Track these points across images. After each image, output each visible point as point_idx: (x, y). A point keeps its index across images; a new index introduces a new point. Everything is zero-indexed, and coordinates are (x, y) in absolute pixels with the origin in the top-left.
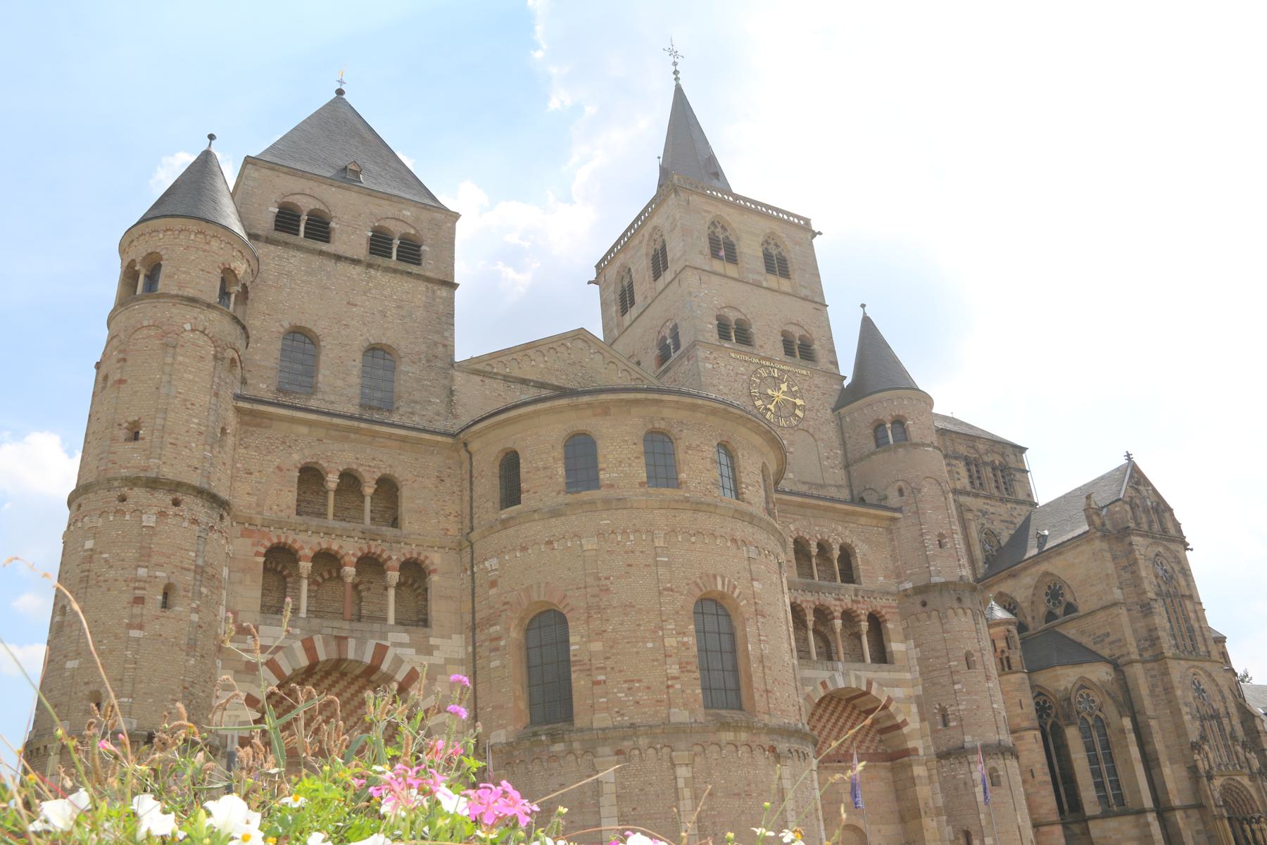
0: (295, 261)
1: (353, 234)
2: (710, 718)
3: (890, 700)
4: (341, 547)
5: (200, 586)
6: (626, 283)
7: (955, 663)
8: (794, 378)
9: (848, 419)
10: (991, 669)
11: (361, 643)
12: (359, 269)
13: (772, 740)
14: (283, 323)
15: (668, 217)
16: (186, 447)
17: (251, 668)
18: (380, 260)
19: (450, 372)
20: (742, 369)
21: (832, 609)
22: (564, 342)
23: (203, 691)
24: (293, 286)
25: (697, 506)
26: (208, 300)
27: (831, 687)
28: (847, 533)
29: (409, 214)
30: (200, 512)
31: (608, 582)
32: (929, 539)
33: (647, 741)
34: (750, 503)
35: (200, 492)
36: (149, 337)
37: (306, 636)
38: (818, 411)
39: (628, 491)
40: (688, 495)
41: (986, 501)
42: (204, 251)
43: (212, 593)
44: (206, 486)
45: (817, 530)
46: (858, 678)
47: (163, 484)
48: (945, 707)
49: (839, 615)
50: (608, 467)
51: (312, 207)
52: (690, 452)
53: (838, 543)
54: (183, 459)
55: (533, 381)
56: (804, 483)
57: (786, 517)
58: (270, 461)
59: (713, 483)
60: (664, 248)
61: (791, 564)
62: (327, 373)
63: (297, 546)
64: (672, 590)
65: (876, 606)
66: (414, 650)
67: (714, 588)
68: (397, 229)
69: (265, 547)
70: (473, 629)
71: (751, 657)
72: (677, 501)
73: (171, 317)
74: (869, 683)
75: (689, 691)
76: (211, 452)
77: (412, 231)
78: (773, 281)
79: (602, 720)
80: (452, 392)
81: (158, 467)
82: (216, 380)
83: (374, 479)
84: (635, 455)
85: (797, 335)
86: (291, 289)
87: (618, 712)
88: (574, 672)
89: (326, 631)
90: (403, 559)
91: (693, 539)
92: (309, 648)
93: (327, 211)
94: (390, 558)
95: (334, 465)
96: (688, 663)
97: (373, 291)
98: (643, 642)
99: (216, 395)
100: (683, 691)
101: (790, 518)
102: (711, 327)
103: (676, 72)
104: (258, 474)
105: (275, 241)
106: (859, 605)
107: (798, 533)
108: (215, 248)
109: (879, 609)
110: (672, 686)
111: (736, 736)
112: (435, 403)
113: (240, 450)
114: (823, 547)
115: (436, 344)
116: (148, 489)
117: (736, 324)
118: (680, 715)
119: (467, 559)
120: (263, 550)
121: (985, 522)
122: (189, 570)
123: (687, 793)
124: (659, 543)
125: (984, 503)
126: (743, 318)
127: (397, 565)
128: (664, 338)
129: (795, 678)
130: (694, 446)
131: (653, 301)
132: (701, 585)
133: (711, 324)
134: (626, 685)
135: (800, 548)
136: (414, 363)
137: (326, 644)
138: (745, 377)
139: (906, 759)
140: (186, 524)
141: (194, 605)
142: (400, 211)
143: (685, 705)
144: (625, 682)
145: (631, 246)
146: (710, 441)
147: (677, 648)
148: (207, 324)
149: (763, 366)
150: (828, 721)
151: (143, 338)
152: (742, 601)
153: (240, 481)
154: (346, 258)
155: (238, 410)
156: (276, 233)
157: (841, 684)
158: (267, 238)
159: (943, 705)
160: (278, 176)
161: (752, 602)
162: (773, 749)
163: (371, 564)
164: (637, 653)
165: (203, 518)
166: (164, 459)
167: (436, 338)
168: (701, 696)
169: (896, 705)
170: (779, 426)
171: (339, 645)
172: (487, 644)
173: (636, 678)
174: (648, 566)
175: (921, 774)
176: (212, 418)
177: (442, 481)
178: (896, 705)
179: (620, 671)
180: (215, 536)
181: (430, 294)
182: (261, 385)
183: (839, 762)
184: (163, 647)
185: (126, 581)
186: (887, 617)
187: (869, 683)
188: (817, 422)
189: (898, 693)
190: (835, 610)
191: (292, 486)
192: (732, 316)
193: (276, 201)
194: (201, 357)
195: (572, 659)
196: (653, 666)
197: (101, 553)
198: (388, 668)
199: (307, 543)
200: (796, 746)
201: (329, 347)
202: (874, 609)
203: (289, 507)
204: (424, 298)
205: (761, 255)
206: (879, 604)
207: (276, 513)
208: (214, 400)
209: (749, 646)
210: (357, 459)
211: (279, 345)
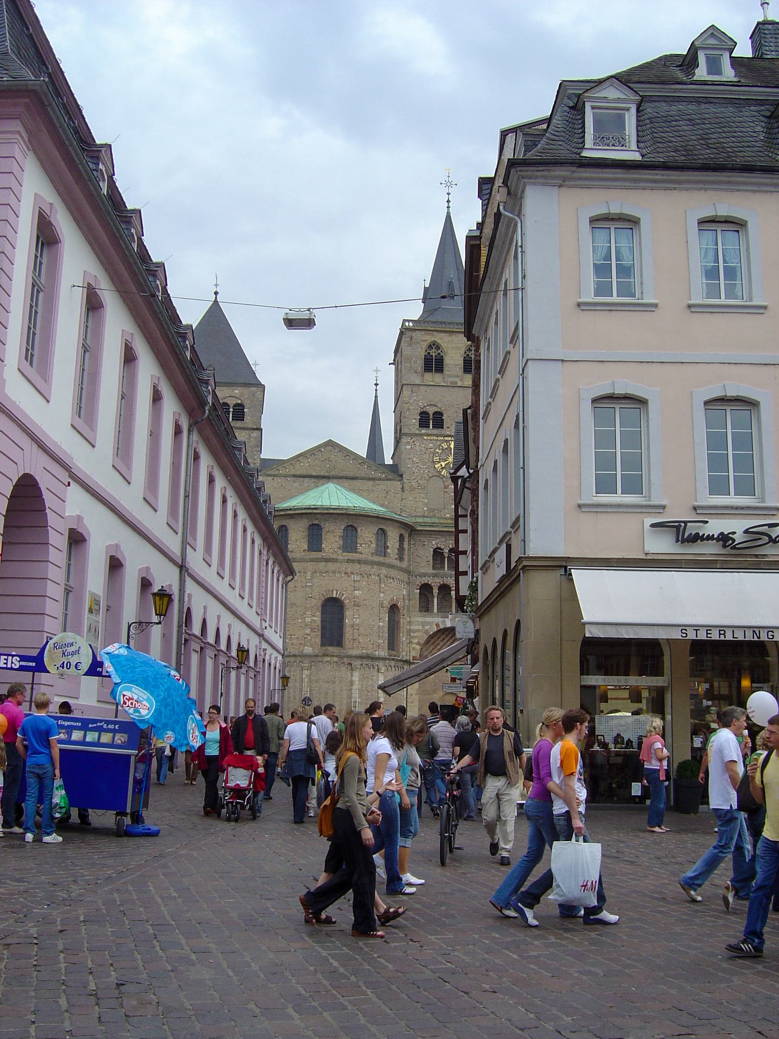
25: (327, 560)
59: (338, 548)
68: (232, 402)
77: (239, 402)
91: (324, 575)
102: (415, 421)
103: (448, 201)
118: (308, 650)
126: (439, 410)
138: (432, 450)
143: (311, 646)
161: (353, 600)
192: (431, 410)
200: (367, 663)
205: (461, 362)
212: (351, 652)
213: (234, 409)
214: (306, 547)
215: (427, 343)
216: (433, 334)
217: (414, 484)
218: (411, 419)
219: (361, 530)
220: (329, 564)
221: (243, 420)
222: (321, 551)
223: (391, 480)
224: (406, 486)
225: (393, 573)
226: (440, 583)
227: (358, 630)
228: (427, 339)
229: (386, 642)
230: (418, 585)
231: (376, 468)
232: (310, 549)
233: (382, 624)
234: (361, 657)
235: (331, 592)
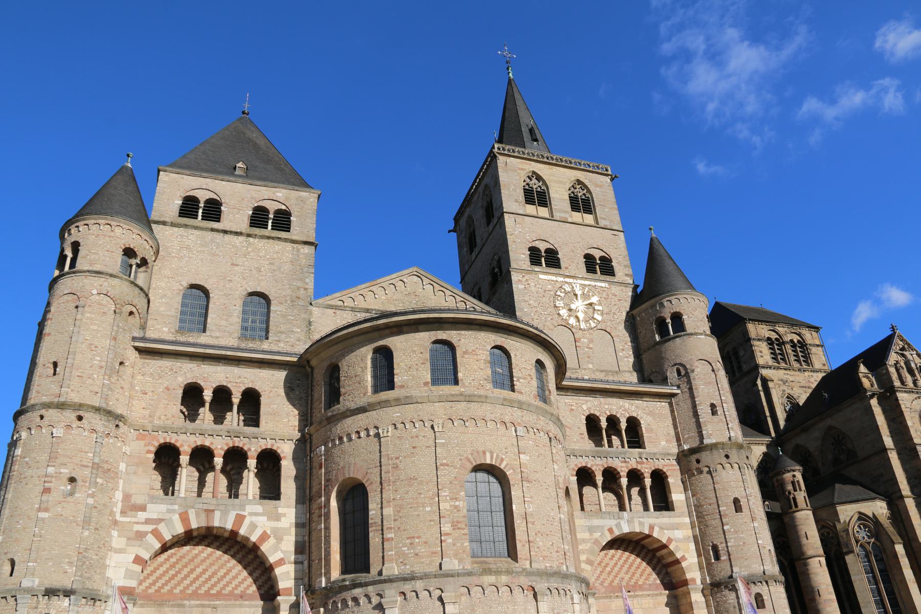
0: (192, 237)
1: (237, 214)
2: (476, 565)
3: (670, 540)
4: (212, 443)
5: (96, 478)
6: (472, 229)
7: (725, 508)
8: (593, 289)
9: (638, 318)
10: (756, 511)
11: (225, 513)
12: (241, 238)
13: (531, 581)
14: (182, 283)
15: (492, 177)
16: (89, 378)
17: (140, 535)
18: (257, 231)
19: (310, 308)
21: (619, 470)
22: (401, 278)
23: (97, 555)
24: (191, 255)
26: (111, 272)
27: (617, 533)
28: (633, 408)
29: (281, 195)
30: (98, 424)
31: (398, 461)
32: (702, 409)
33: (422, 585)
34: (521, 393)
35: (97, 410)
36: (67, 301)
37: (183, 511)
38: (614, 314)
39: (415, 390)
40: (464, 390)
41: (786, 372)
42: (110, 237)
43: (107, 482)
44: (104, 406)
45: (603, 408)
46: (641, 524)
47: (69, 405)
48: (716, 545)
49: (626, 474)
50: (401, 372)
51: (208, 198)
52: (466, 356)
53: (624, 417)
54: (86, 387)
55: (375, 310)
56: (602, 371)
57: (579, 400)
58: (161, 384)
59: (485, 379)
60: (491, 200)
61: (583, 436)
62: (214, 316)
63: (178, 444)
64: (448, 465)
65: (658, 465)
66: (266, 518)
67: (483, 462)
68: (272, 207)
69: (155, 446)
70: (310, 500)
72: (453, 395)
73: (83, 286)
74: (652, 528)
75: (459, 545)
76: (109, 380)
77: (284, 207)
78: (577, 216)
79: (392, 569)
80: (310, 323)
81: (67, 394)
82: (115, 328)
83: (239, 392)
84: (421, 362)
85: (597, 257)
86: (189, 257)
87: (402, 562)
88: (372, 531)
89: (197, 506)
90: (260, 450)
92: (184, 518)
93: (218, 199)
94: (250, 449)
95: (209, 384)
96: (458, 522)
97: (252, 254)
98: (422, 507)
99: (115, 339)
100: (454, 545)
101: (584, 400)
104: (151, 394)
105: (178, 224)
106: (643, 466)
107: (589, 411)
108: (118, 234)
109: (661, 468)
111: (497, 579)
112: (297, 332)
113: (138, 377)
114: (613, 421)
115: (298, 288)
116: (59, 410)
117: (545, 252)
119: (308, 448)
120: (154, 449)
121: (785, 388)
122: (87, 466)
125: (784, 374)
126: (552, 247)
127: (256, 455)
128: (494, 269)
129: (561, 529)
131: (486, 241)
132: (472, 460)
133: (523, 254)
135: (592, 422)
136: (281, 304)
137: (197, 515)
138: (552, 293)
139: (685, 587)
140: (86, 433)
141: (90, 492)
142: (274, 193)
143: (455, 555)
144: (408, 538)
145: (473, 201)
146: (485, 346)
148: (109, 289)
149: (567, 283)
150: (620, 559)
151: (63, 303)
152: (510, 469)
153: (138, 400)
154: (231, 232)
155: (136, 348)
156: (180, 218)
157: (626, 529)
158: (172, 223)
159: (715, 543)
160: (183, 178)
163: (236, 457)
164: (418, 515)
165: (100, 428)
166: (72, 387)
167: (299, 284)
168: (468, 548)
169: (676, 544)
170: (580, 329)
171: (207, 516)
172: (317, 511)
173: (417, 535)
174: (429, 447)
175: (698, 600)
176: (111, 356)
177: (293, 390)
178: (676, 544)
179: (404, 530)
180: (111, 441)
181: (295, 252)
182: (164, 329)
183: (629, 592)
184: (63, 524)
185: (39, 477)
186: (668, 474)
187: (652, 528)
188: (614, 322)
189: (678, 534)
190: (622, 471)
191: (177, 401)
192: (543, 247)
193: (180, 196)
194: (104, 313)
195: (370, 521)
196: (430, 525)
197: (24, 458)
198: (245, 532)
199: (186, 444)
200: (556, 585)
201: (216, 297)
202: (657, 468)
203: (173, 416)
204: (290, 256)
205: (568, 198)
206: (659, 464)
207: (164, 421)
208: (113, 343)
210: (227, 378)
211: (179, 299)
214: (428, 377)
216: (531, 165)
221: (289, 231)
226: (602, 465)
228: (524, 167)
232: (436, 381)
235: (481, 454)
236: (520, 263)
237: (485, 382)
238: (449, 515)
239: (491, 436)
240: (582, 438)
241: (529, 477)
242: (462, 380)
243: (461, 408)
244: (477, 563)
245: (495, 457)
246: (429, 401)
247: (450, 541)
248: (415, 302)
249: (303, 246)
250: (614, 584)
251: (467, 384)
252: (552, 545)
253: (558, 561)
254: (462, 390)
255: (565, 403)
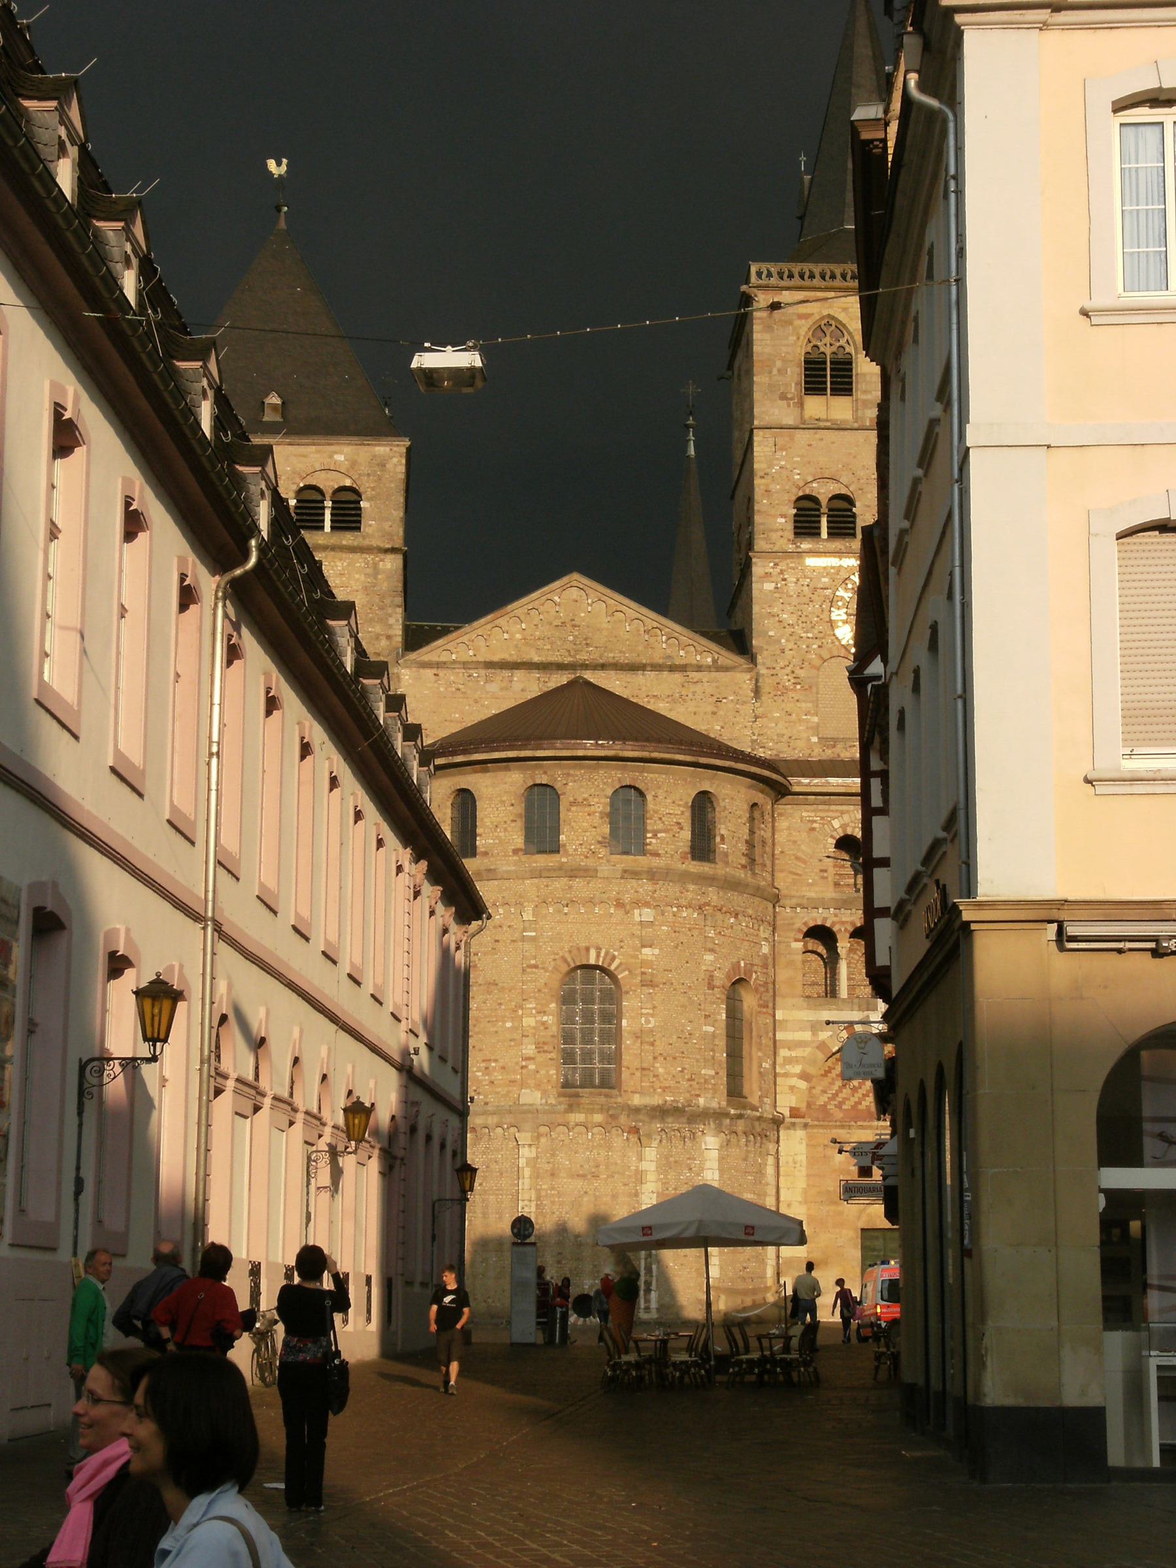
2: (562, 1099)
20: (824, 580)
22: (549, 596)
25: (573, 873)
34: (658, 855)
52: (573, 809)
57: (829, 811)
59: (599, 842)
64: (536, 966)
68: (328, 483)
71: (625, 1034)
72: (549, 870)
75: (543, 1072)
77: (348, 483)
84: (511, 818)
91: (566, 910)
96: (545, 1043)
107: (844, 830)
110: (526, 1067)
118: (531, 1097)
123: (527, 1172)
124: (528, 916)
126: (844, 491)
130: (580, 800)
132: (569, 959)
133: (782, 516)
134: (483, 1065)
138: (828, 592)
142: (331, 457)
143: (538, 1086)
144: (483, 1061)
146: (603, 790)
147: (534, 1028)
152: (624, 971)
161: (638, 971)
162: (635, 1131)
164: (496, 1032)
173: (492, 1058)
174: (514, 941)
179: (480, 1050)
181: (369, 571)
192: (824, 492)
200: (677, 1126)
204: (363, 577)
209: (624, 1022)
212: (637, 1100)
213: (334, 502)
214: (519, 840)
215: (810, 322)
217: (787, 680)
218: (775, 516)
219: (655, 796)
220: (577, 883)
221: (359, 529)
222: (558, 852)
223: (726, 669)
224: (767, 684)
225: (737, 900)
226: (852, 923)
227: (652, 1044)
229: (723, 1074)
230: (799, 930)
231: (691, 642)
233: (711, 1029)
234: (661, 1112)
235: (583, 952)
236: (774, 536)
237: (598, 846)
238: (534, 1035)
239: (600, 925)
240: (823, 878)
241: (655, 980)
242: (564, 845)
243: (559, 884)
244: (564, 1095)
245: (602, 954)
246: (518, 878)
247: (532, 1067)
248: (571, 638)
249: (382, 556)
250: (860, 1107)
251: (571, 851)
252: (681, 1072)
253: (688, 1092)
254: (564, 860)
255: (802, 817)
